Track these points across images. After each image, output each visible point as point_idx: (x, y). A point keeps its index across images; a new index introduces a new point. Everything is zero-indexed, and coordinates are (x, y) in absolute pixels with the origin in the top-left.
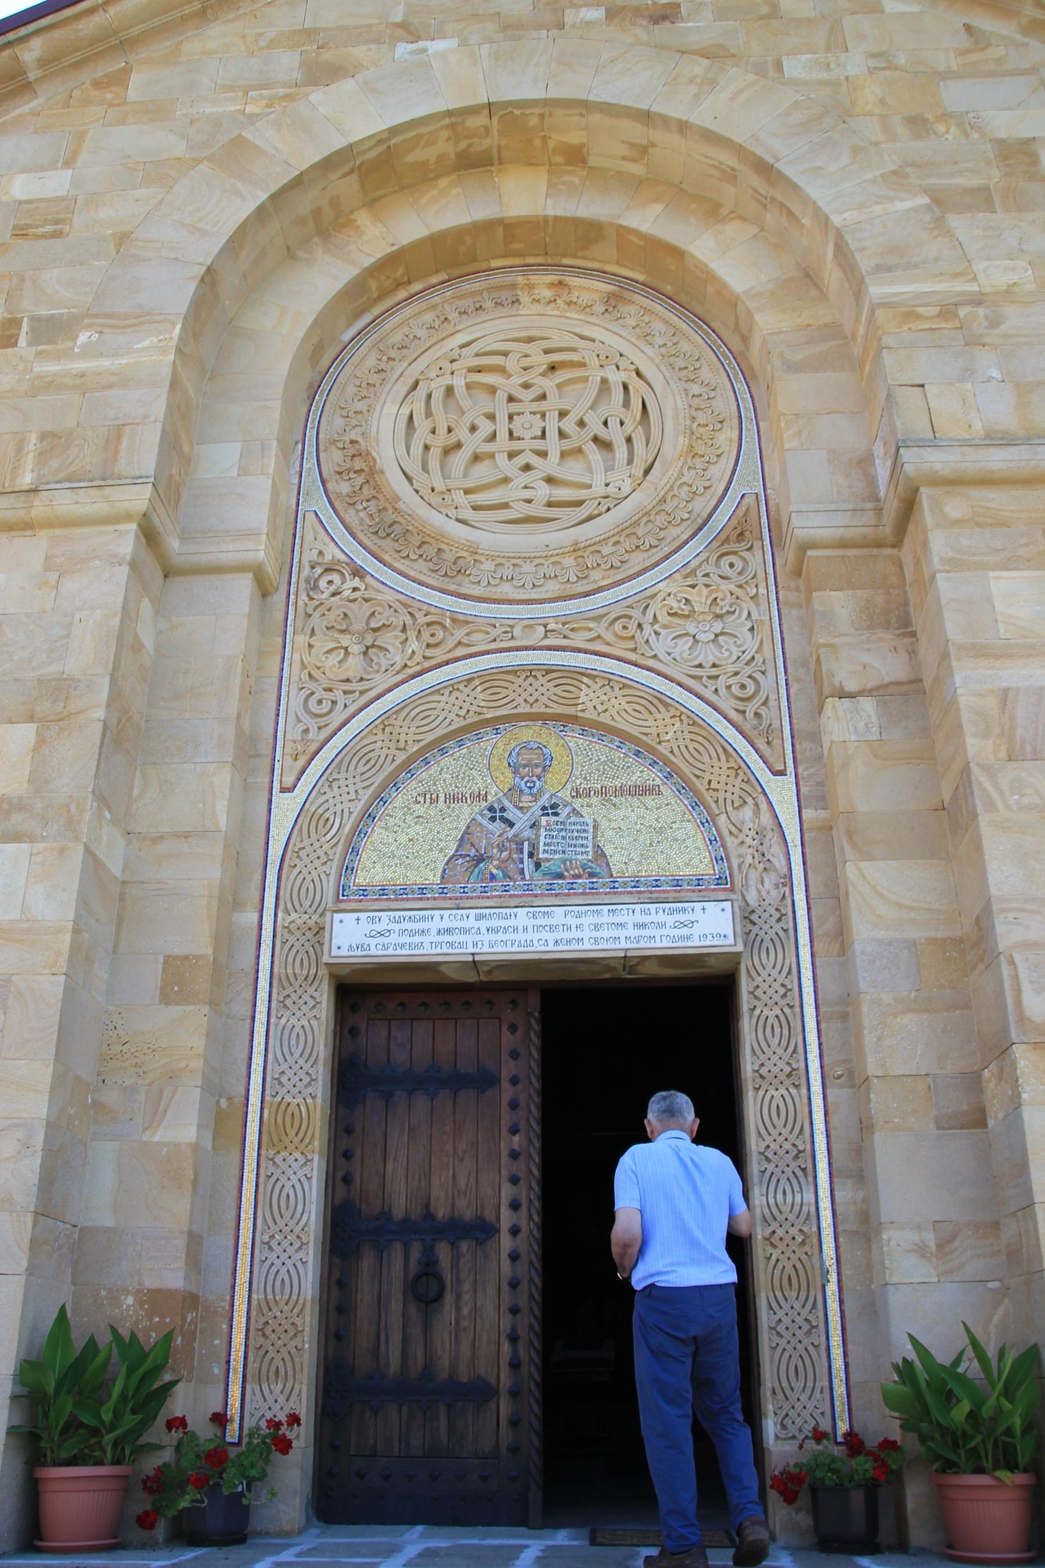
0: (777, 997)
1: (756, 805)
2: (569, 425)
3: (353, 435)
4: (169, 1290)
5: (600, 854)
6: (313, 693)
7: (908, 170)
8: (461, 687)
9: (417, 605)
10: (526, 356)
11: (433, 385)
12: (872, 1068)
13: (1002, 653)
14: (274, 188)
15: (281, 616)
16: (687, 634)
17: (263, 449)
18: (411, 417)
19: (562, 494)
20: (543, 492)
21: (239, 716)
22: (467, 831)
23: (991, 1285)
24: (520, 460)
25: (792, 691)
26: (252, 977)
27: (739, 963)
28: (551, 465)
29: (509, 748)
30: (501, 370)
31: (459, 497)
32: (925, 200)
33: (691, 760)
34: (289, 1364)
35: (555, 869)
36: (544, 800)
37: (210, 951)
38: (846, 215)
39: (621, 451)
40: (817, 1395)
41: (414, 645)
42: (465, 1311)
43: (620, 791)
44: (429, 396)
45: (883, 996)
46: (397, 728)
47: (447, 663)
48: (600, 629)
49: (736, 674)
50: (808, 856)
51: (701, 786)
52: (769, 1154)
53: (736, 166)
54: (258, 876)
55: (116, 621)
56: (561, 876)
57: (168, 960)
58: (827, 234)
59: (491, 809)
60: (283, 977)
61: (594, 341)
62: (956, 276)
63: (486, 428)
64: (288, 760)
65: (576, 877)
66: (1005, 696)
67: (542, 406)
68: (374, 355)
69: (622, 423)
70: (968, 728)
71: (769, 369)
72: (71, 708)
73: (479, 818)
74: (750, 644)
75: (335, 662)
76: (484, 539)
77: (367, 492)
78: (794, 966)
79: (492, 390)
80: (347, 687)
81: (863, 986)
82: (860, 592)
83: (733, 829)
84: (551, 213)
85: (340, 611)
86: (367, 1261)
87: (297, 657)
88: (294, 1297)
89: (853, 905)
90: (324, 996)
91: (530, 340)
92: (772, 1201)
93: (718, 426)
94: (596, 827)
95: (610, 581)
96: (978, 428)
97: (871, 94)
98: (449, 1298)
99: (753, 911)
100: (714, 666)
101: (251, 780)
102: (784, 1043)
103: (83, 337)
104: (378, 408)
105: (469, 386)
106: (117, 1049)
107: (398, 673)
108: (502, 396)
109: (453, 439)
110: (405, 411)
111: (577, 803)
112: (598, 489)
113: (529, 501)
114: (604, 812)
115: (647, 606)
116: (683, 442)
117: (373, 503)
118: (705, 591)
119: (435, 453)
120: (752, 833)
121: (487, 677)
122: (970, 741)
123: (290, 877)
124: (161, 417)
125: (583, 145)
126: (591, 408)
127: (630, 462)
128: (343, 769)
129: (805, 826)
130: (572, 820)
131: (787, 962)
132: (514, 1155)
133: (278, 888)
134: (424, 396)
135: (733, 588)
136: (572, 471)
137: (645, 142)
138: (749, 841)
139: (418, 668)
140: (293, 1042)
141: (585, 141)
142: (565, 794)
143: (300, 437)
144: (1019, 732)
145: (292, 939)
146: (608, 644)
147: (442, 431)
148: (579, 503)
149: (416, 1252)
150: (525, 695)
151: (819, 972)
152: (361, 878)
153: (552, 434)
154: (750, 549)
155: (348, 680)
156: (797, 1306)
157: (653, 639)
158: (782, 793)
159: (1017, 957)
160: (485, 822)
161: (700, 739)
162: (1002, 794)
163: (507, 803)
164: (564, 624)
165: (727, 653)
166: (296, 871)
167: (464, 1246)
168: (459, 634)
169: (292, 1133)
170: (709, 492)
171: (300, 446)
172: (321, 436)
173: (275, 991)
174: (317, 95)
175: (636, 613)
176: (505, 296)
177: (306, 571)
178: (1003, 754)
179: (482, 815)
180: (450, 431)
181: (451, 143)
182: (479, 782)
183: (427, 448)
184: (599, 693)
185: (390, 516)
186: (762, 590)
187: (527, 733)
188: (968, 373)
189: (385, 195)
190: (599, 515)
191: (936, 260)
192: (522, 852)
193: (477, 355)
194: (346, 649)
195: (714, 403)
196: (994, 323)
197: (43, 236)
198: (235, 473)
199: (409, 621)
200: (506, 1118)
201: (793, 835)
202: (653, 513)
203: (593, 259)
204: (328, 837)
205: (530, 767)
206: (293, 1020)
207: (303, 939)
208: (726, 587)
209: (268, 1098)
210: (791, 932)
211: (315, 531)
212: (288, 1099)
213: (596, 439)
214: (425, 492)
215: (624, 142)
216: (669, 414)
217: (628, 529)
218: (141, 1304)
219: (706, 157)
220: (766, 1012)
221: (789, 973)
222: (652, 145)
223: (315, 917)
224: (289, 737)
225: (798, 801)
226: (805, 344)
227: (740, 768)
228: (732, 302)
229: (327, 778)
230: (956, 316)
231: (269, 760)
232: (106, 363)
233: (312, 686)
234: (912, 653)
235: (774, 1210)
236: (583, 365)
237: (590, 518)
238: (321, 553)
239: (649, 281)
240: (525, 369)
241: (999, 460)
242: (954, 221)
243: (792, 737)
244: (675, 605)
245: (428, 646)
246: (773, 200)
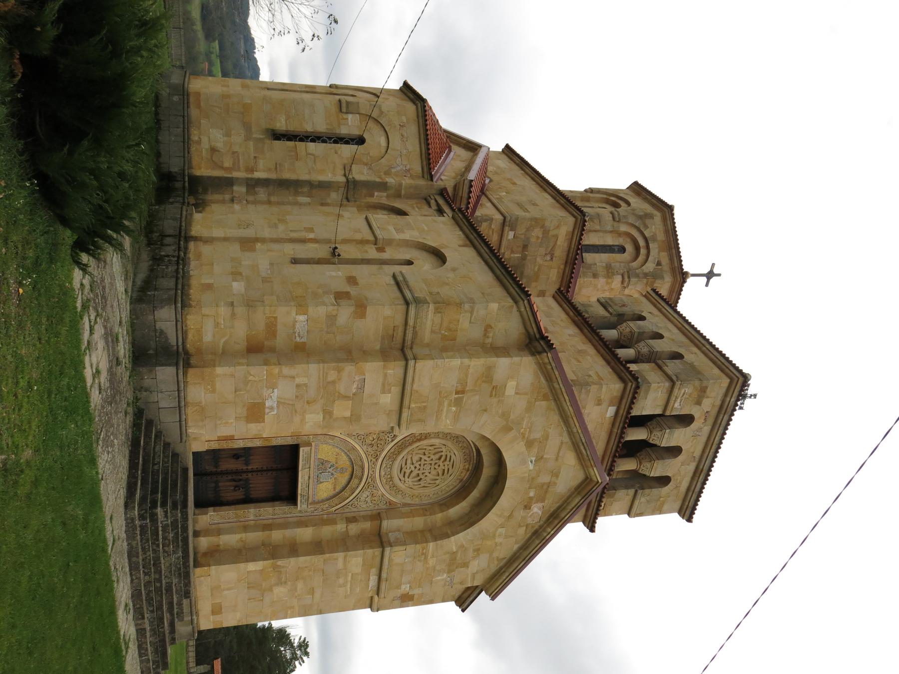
19: (407, 475)
20: (408, 472)
32: (455, 550)
66: (337, 559)
97: (489, 543)
103: (454, 409)
112: (407, 479)
174: (522, 443)
187: (350, 469)
205: (342, 471)
241: (386, 561)
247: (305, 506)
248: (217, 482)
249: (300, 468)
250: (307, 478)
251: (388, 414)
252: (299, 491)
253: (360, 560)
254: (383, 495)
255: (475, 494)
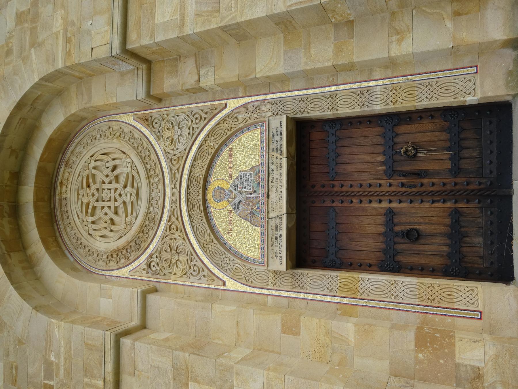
0: (304, 104)
1: (236, 113)
2: (107, 180)
3: (105, 257)
4: (416, 338)
5: (252, 169)
6: (191, 273)
7: (22, 56)
8: (192, 219)
9: (163, 234)
10: (83, 195)
11: (91, 228)
12: (330, 64)
13: (183, 17)
14: (9, 283)
15: (164, 284)
16: (178, 138)
17: (103, 290)
18: (101, 236)
20: (129, 189)
21: (196, 301)
22: (242, 217)
23: (414, 14)
24: (117, 197)
25: (199, 101)
26: (291, 299)
27: (292, 118)
28: (120, 186)
29: (214, 202)
30: (88, 204)
31: (128, 219)
33: (221, 137)
34: (445, 290)
35: (256, 186)
36: (232, 189)
37: (280, 315)
38: (35, 77)
39: (117, 162)
40: (457, 81)
41: (176, 235)
42: (422, 220)
43: (230, 162)
44: (95, 230)
45: (303, 61)
46: (205, 242)
47: (183, 224)
48: (174, 169)
49: (192, 121)
50: (255, 94)
51: (229, 133)
52: (361, 104)
53: (19, 117)
54: (254, 295)
55: (154, 347)
56: (259, 183)
57: (284, 332)
58: (43, 85)
59: (235, 209)
60: (292, 287)
61: (80, 172)
62: (57, 38)
63: (106, 210)
64: (214, 283)
65: (259, 176)
67: (100, 190)
68: (79, 249)
69: (108, 162)
70: (208, 28)
71: (91, 109)
72: (184, 367)
73: (238, 213)
74: (182, 116)
75: (181, 265)
76: (143, 210)
77: (124, 252)
78: (293, 98)
79: (94, 208)
80: (189, 260)
81: (299, 69)
82: (165, 76)
83: (245, 121)
84: (33, 185)
85: (164, 263)
86: (401, 258)
87: (178, 279)
88: (417, 287)
89: (271, 74)
90: (299, 271)
91: (78, 194)
92: (379, 103)
93: (111, 129)
94: (242, 171)
95: (159, 166)
96: (106, 28)
98: (417, 227)
99: (274, 114)
100: (189, 129)
101: (220, 298)
102: (320, 101)
103: (53, 358)
104: (97, 248)
105: (93, 215)
106: (317, 355)
107: (186, 242)
108: (96, 204)
109: (109, 221)
110: (98, 238)
111: (234, 178)
112: (128, 170)
113: (131, 194)
114: (237, 168)
115: (169, 153)
116: (115, 141)
117: (129, 250)
118: (164, 132)
119: (113, 227)
120: (246, 114)
121: (189, 209)
122: (212, 27)
123: (255, 283)
124: (83, 328)
125: (10, 172)
126: (102, 173)
127: (120, 159)
128: (218, 262)
129: (244, 95)
130: (240, 179)
131: (291, 100)
132: (361, 202)
133: (259, 288)
134: (94, 231)
135: (163, 123)
136: (122, 179)
137: (10, 150)
138: (249, 116)
139: (184, 234)
140: (316, 284)
141: (8, 172)
142: (231, 182)
143: (104, 277)
144: (210, 9)
145: (278, 283)
146: (180, 166)
147: (105, 225)
148: (133, 177)
149: (398, 240)
150: (196, 196)
151: (295, 89)
152: (257, 257)
153: (110, 186)
154: (151, 117)
155: (187, 260)
156: (420, 91)
157: (179, 150)
158: (233, 104)
159: (289, 4)
160: (239, 211)
161: (213, 134)
162: (231, 14)
163: (233, 203)
164: (172, 182)
165: (185, 123)
166: (253, 281)
167: (396, 221)
168: (173, 219)
169: (351, 285)
170: (133, 132)
171: (107, 277)
172: (104, 269)
173: (296, 290)
175: (170, 156)
176: (64, 204)
177: (149, 275)
178: (217, 14)
179: (237, 212)
180: (106, 222)
181: (4, 219)
182: (225, 213)
183: (111, 231)
184: (196, 169)
185: (133, 244)
186: (165, 113)
187: (209, 196)
188: (89, 32)
189: (22, 244)
190: (137, 169)
191: (52, 45)
192: (250, 197)
193: (82, 212)
194: (177, 261)
195: (104, 130)
196: (73, 24)
197: (16, 374)
198: (111, 300)
199: (168, 238)
200: (346, 205)
201: (247, 100)
202: (138, 151)
203: (54, 172)
204: (242, 268)
206: (308, 283)
207: (278, 279)
208: (163, 125)
209: (337, 295)
210: (281, 99)
211: (136, 272)
212: (338, 286)
213: (113, 171)
214: (126, 231)
215: (9, 158)
216: (105, 146)
217: (142, 159)
218: (422, 351)
219: (16, 128)
220: (309, 108)
221: (295, 99)
222: (11, 147)
223: (270, 274)
224: (206, 283)
225: (236, 98)
226: (82, 95)
227: (224, 120)
228: (68, 122)
229: (221, 267)
230: (70, 37)
231: (213, 290)
232: (62, 349)
233: (188, 273)
234: (186, 57)
235: (382, 102)
236: (88, 176)
237: (138, 173)
238: (144, 270)
239: (62, 153)
240: (88, 196)
241: (118, 20)
242: (40, 39)
243: (214, 101)
244: (168, 143)
245: (177, 230)
246: (32, 105)
247: (275, 123)
248: (456, 171)
249: (285, 218)
250: (273, 195)
251: (135, 369)
252: (284, 160)
253: (159, 19)
254: (158, 138)
255: (37, 151)
